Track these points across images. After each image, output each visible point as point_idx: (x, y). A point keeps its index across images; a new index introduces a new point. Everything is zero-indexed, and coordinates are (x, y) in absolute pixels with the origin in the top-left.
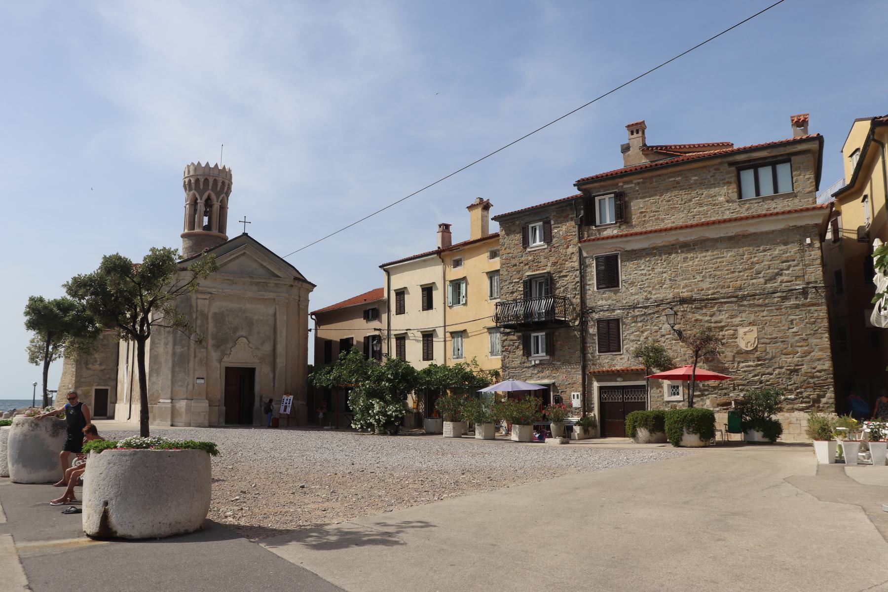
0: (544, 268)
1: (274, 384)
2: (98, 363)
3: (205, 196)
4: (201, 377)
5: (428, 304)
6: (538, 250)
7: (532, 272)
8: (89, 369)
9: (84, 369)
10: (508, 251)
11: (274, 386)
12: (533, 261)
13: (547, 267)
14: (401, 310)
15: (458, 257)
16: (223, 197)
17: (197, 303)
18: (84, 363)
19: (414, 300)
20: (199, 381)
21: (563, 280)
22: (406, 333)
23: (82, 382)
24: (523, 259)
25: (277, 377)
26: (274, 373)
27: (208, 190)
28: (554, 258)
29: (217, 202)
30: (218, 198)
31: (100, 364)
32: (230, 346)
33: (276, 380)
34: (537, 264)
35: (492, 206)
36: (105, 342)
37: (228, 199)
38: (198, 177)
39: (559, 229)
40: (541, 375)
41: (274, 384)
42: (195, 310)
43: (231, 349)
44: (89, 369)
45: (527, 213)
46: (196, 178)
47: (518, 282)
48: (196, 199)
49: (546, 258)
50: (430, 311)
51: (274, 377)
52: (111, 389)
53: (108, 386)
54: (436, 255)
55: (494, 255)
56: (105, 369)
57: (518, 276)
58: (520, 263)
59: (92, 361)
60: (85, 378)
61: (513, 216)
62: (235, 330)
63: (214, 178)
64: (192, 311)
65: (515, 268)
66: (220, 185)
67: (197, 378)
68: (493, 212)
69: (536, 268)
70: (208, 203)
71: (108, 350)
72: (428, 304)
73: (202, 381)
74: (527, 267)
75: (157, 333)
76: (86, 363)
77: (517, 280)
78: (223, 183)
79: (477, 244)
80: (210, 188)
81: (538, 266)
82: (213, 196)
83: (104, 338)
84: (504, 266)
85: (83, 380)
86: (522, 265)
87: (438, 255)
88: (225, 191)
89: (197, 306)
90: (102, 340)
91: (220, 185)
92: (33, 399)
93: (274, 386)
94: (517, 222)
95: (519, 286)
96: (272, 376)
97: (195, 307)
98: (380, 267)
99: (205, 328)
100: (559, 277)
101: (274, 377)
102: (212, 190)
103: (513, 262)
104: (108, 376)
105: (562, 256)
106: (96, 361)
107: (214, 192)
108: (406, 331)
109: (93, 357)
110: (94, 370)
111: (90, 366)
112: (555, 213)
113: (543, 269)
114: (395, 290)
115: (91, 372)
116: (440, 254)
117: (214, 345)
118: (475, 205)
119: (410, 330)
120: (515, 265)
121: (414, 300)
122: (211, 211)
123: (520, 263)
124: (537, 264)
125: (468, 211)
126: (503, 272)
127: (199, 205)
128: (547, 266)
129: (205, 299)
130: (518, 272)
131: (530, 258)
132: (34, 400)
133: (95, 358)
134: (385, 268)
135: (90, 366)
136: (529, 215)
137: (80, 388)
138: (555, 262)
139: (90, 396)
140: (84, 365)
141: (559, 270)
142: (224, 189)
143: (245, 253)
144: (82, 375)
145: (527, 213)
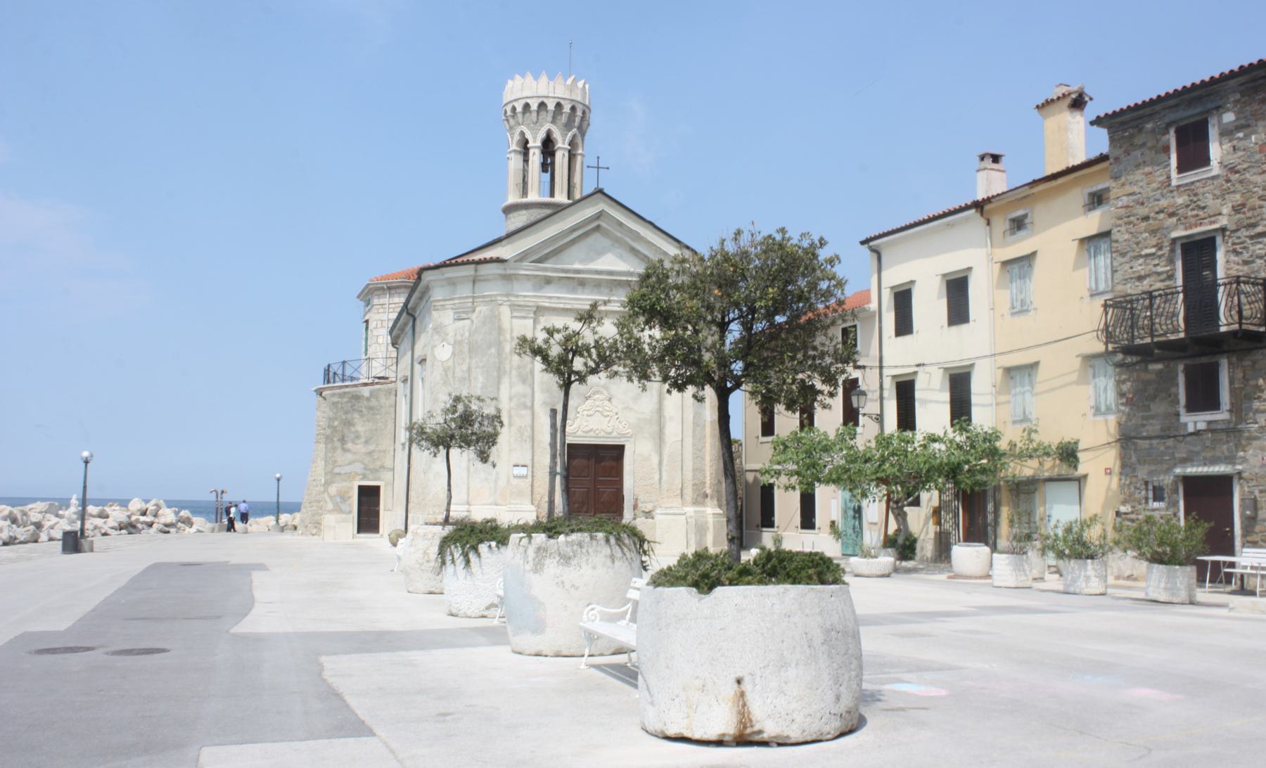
0: (1213, 219)
1: (660, 474)
2: (363, 440)
3: (542, 135)
4: (523, 463)
5: (958, 312)
6: (1198, 181)
7: (1186, 229)
8: (348, 450)
9: (339, 451)
10: (1128, 189)
11: (660, 479)
12: (1187, 206)
13: (1220, 217)
14: (904, 326)
15: (1020, 213)
16: (574, 136)
17: (511, 323)
18: (339, 440)
20: (518, 471)
21: (1260, 243)
22: (915, 373)
23: (337, 474)
24: (1164, 203)
25: (665, 463)
26: (661, 455)
28: (1238, 196)
29: (564, 140)
30: (564, 136)
31: (366, 442)
32: (576, 405)
33: (664, 468)
34: (1195, 212)
35: (1091, 99)
36: (373, 403)
37: (583, 140)
39: (1247, 131)
40: (1209, 454)
41: (660, 474)
42: (508, 336)
43: (577, 408)
44: (348, 450)
45: (1172, 102)
47: (1153, 254)
48: (527, 142)
49: (1216, 197)
50: (964, 327)
51: (660, 463)
52: (385, 486)
53: (378, 479)
54: (973, 211)
55: (1097, 200)
56: (374, 451)
57: (1154, 241)
58: (1157, 213)
59: (352, 436)
60: (340, 466)
61: (1141, 112)
63: (558, 100)
64: (501, 338)
65: (1144, 224)
66: (567, 109)
67: (515, 466)
68: (1096, 109)
69: (1193, 220)
70: (548, 146)
71: (378, 417)
72: (958, 312)
73: (523, 471)
74: (1174, 220)
75: (442, 382)
76: (343, 440)
77: (1153, 250)
78: (573, 109)
79: (1060, 181)
81: (1197, 216)
82: (556, 134)
83: (371, 395)
84: (1120, 222)
85: (337, 470)
86: (1162, 216)
87: (977, 211)
88: (576, 124)
89: (512, 331)
90: (368, 399)
91: (567, 109)
92: (275, 500)
93: (660, 479)
94: (1149, 126)
95: (1156, 262)
96: (655, 460)
97: (509, 332)
98: (863, 243)
99: (528, 370)
100: (1252, 237)
101: (660, 463)
103: (1142, 211)
104: (378, 463)
105: (1256, 189)
106: (358, 437)
108: (916, 369)
109: (353, 429)
110: (355, 453)
111: (349, 446)
112: (1238, 96)
113: (1212, 223)
114: (892, 288)
115: (349, 456)
116: (982, 208)
117: (544, 403)
118: (1052, 100)
119: (923, 365)
120: (1146, 218)
122: (553, 163)
123: (1157, 213)
124: (1195, 212)
125: (1037, 114)
126: (1121, 235)
127: (531, 152)
128: (1220, 214)
129: (525, 318)
130: (1153, 232)
131: (1180, 201)
132: (278, 502)
133: (357, 431)
134: (871, 244)
135: (349, 446)
136: (1176, 106)
137: (334, 485)
138: (1239, 205)
139: (350, 497)
140: (338, 444)
141: (1252, 221)
142: (574, 121)
143: (598, 227)
144: (335, 462)
145: (1172, 102)
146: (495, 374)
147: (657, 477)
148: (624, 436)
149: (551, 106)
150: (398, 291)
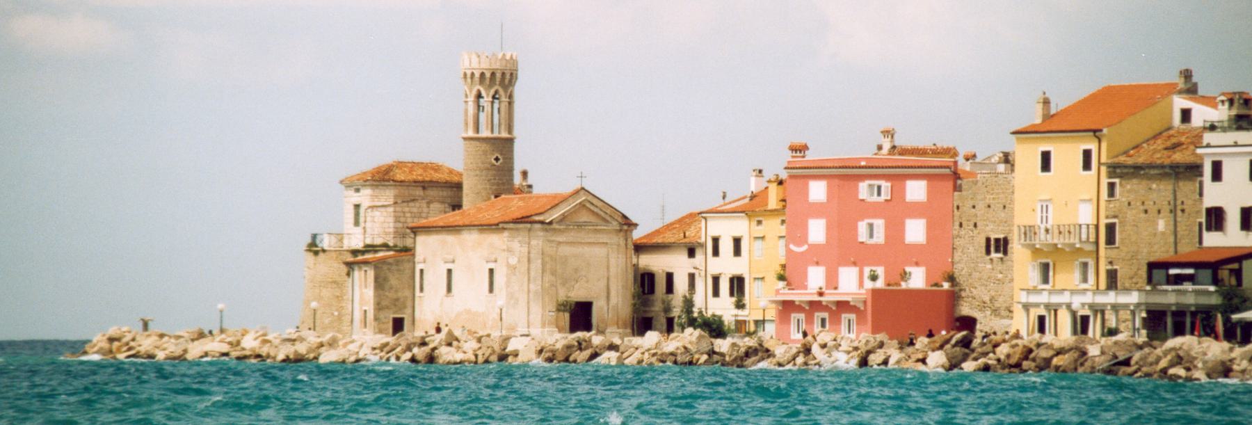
5: (737, 252)
14: (716, 252)
15: (760, 219)
19: (726, 246)
26: (608, 305)
27: (496, 84)
30: (506, 91)
38: (484, 71)
46: (481, 71)
53: (404, 313)
62: (576, 270)
66: (508, 77)
72: (737, 252)
80: (498, 83)
91: (508, 77)
96: (606, 308)
102: (500, 85)
106: (391, 288)
107: (502, 87)
121: (726, 246)
146: (541, 272)
147: (606, 316)
148: (594, 298)
149: (498, 75)
150: (389, 187)
